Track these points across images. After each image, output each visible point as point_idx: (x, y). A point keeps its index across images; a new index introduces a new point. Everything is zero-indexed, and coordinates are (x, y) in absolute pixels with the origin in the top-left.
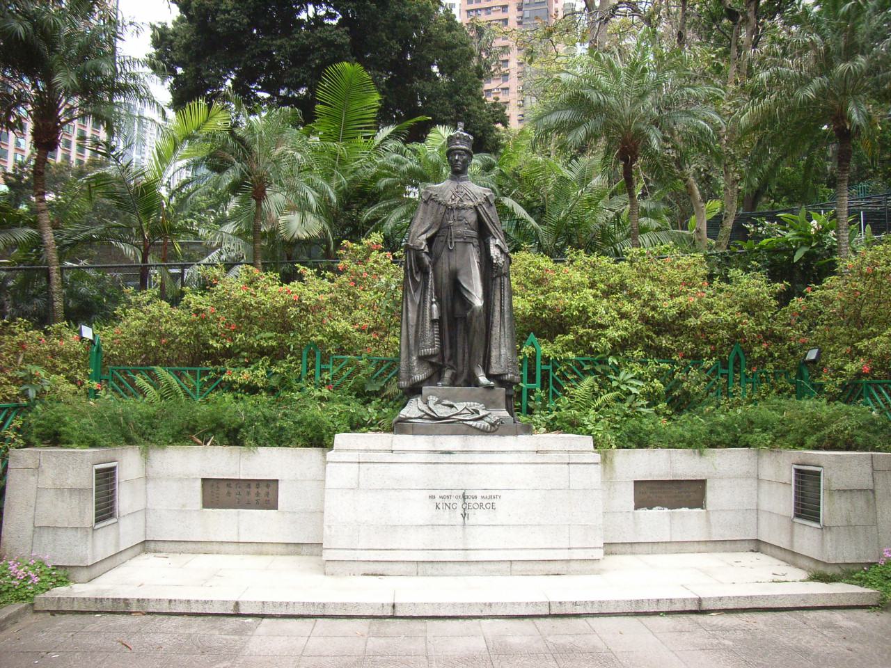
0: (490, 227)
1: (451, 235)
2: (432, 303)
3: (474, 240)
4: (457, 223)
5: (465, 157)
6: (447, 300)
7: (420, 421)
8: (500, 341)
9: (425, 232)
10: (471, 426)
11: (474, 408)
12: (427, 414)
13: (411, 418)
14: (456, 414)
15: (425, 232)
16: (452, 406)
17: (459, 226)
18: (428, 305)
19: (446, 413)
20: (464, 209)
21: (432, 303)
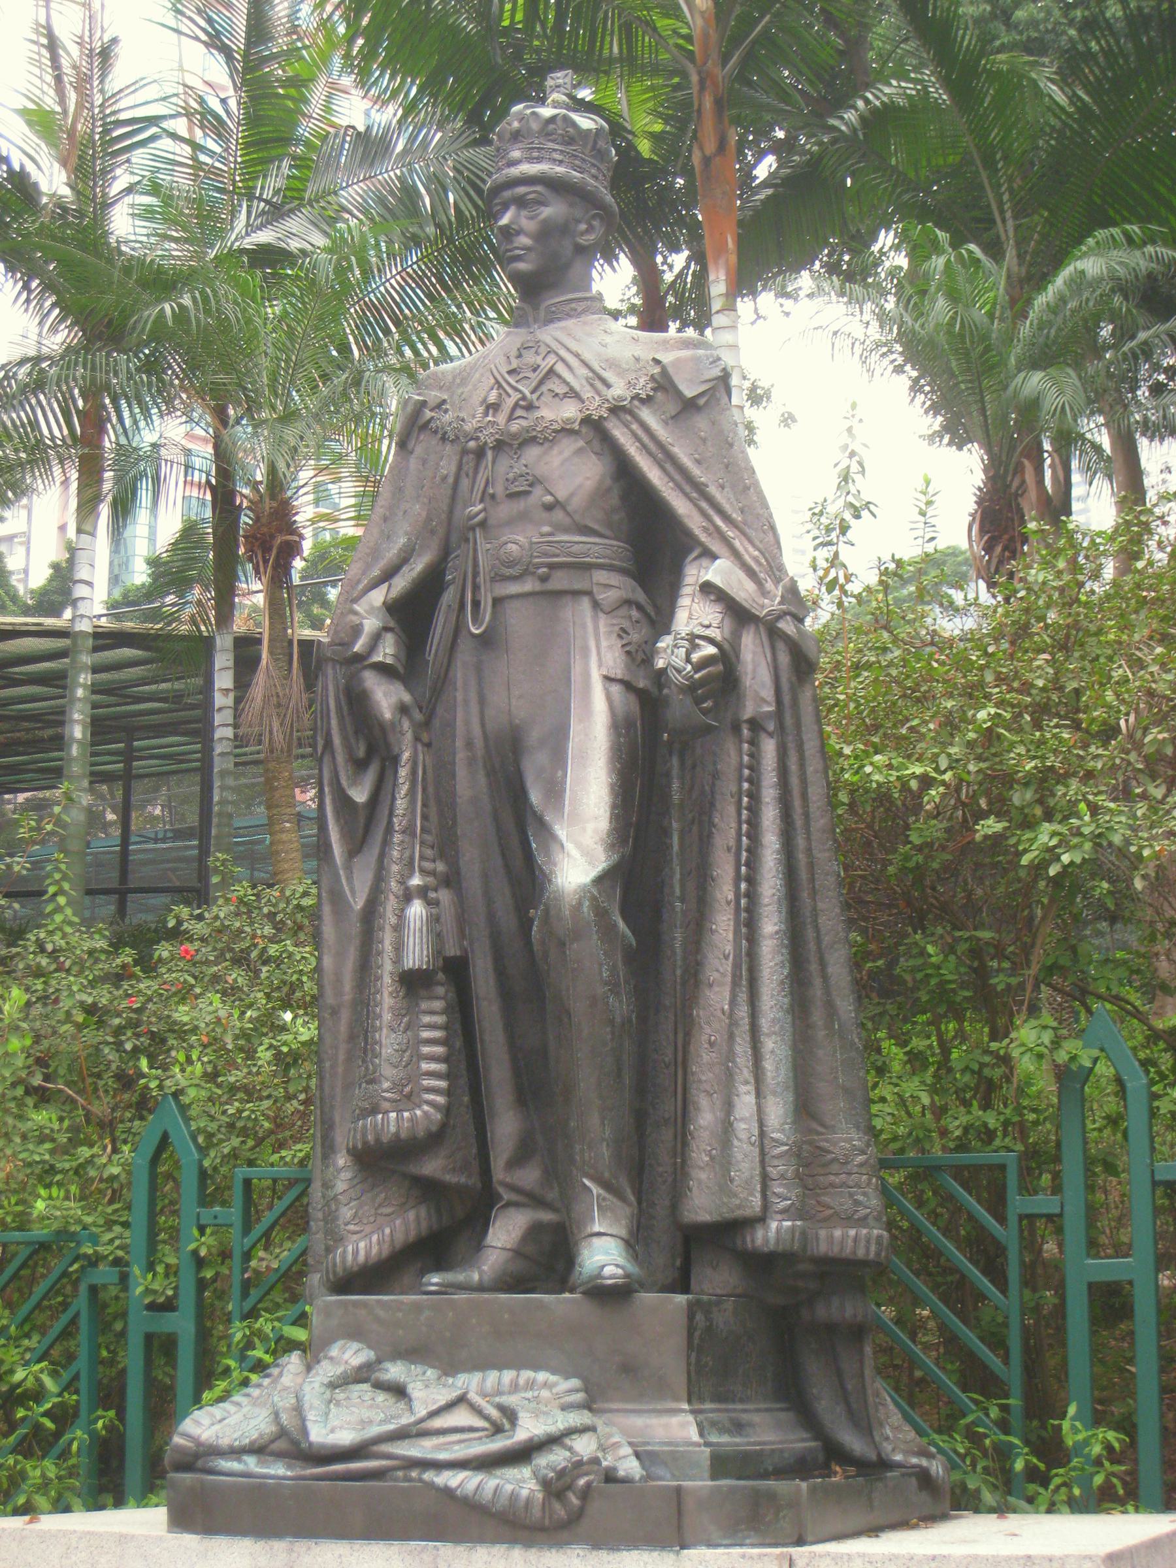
0: (680, 505)
1: (476, 574)
3: (600, 576)
4: (505, 510)
5: (546, 212)
6: (485, 876)
7: (251, 1463)
8: (730, 1056)
9: (388, 576)
10: (448, 1492)
11: (506, 1400)
14: (401, 1435)
15: (388, 576)
16: (399, 1391)
17: (510, 522)
18: (391, 904)
19: (365, 1423)
20: (533, 440)
21: (407, 897)
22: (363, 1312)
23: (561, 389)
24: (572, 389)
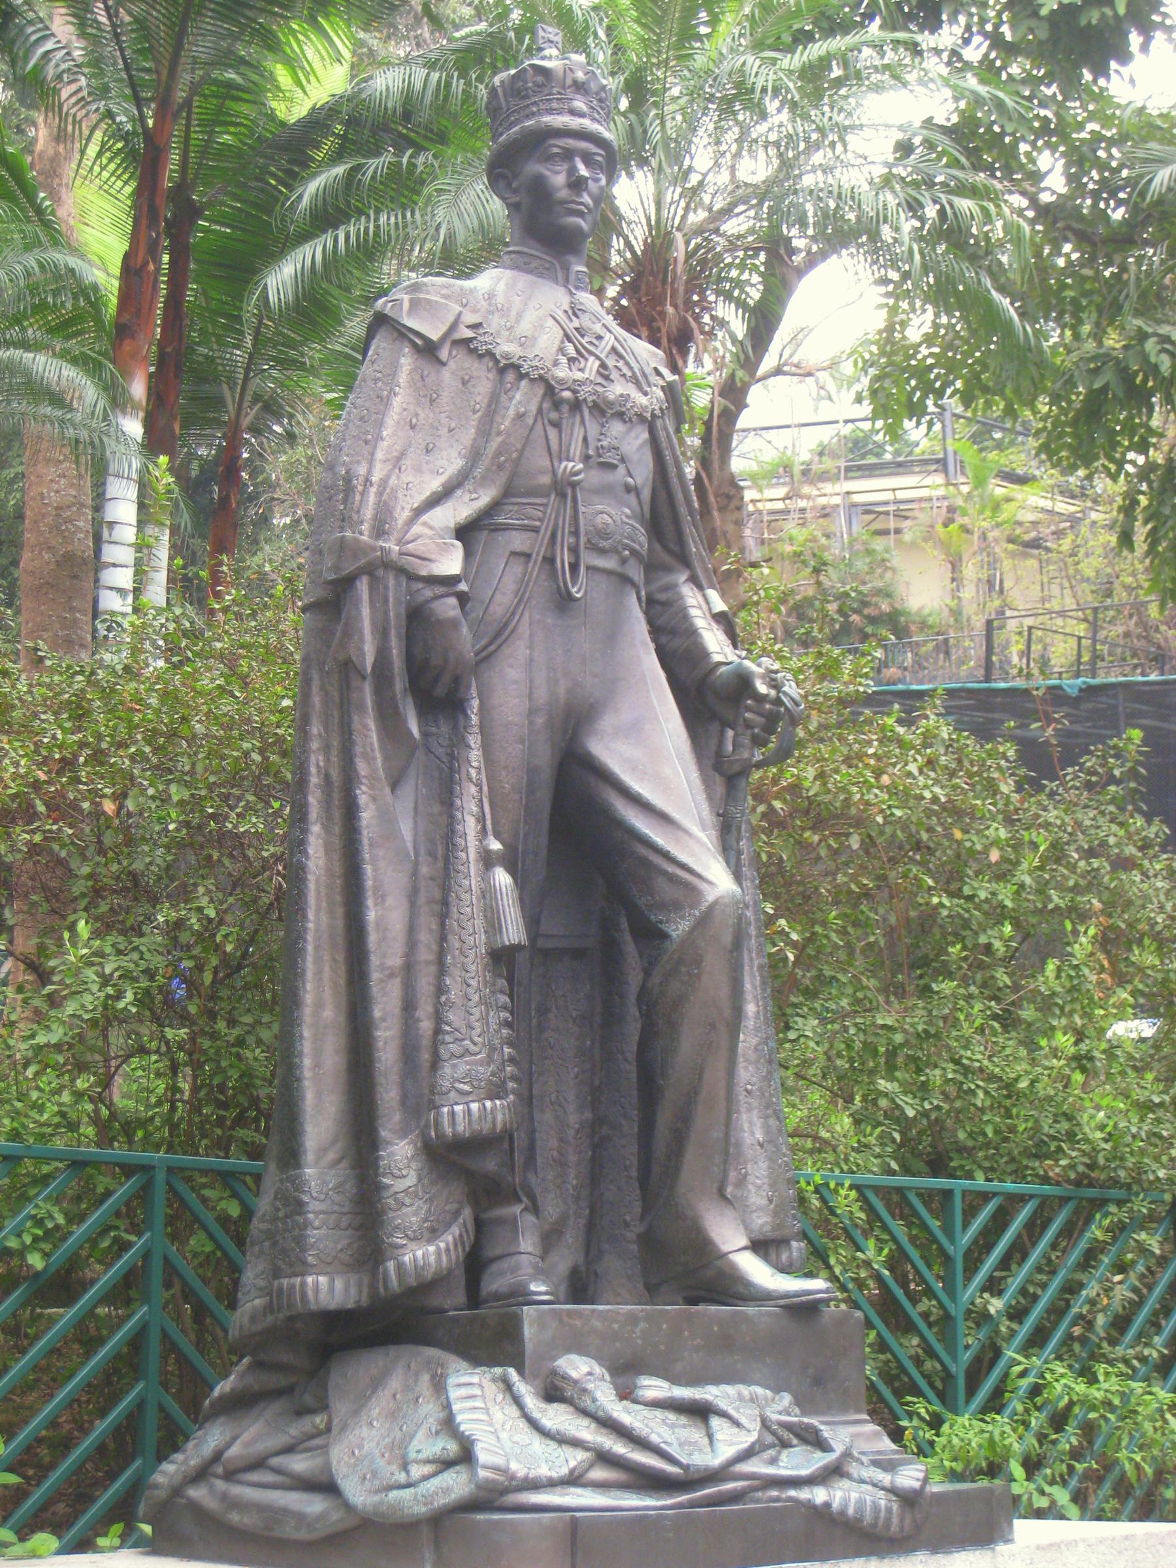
2: (488, 860)
4: (596, 477)
12: (604, 1458)
13: (535, 1485)
22: (578, 1323)
23: (629, 374)
24: (634, 373)
